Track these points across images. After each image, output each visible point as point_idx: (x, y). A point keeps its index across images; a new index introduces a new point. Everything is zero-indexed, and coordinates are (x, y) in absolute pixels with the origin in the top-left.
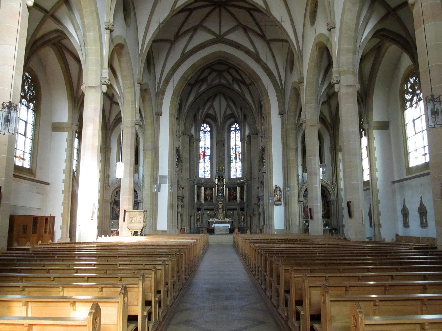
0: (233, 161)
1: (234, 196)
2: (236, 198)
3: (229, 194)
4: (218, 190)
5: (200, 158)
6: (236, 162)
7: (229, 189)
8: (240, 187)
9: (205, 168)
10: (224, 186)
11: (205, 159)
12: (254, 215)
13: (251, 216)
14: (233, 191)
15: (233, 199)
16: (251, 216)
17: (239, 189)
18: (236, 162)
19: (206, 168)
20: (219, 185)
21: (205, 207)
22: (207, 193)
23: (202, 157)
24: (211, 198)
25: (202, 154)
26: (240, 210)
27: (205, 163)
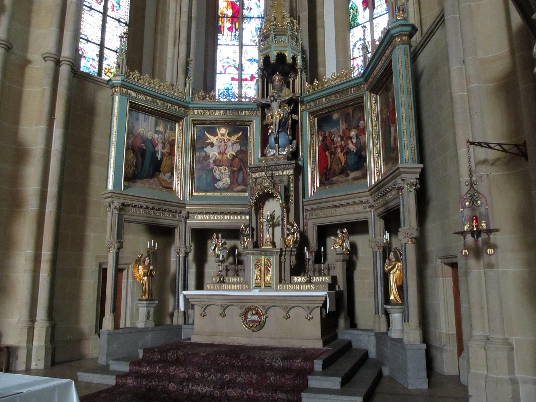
0: (360, 20)
1: (348, 153)
2: (359, 161)
3: (326, 148)
4: (265, 128)
5: (219, 30)
6: (372, 18)
7: (324, 119)
8: (374, 90)
9: (240, 68)
10: (295, 111)
11: (241, 29)
12: (477, 253)
13: (454, 266)
14: (343, 126)
15: (344, 171)
16: (454, 266)
17: (372, 104)
18: (372, 18)
19: (246, 64)
20: (268, 106)
21: (200, 220)
22: (213, 153)
23: (227, 24)
24: (232, 175)
25: (230, 12)
26: (380, 224)
27: (241, 45)
